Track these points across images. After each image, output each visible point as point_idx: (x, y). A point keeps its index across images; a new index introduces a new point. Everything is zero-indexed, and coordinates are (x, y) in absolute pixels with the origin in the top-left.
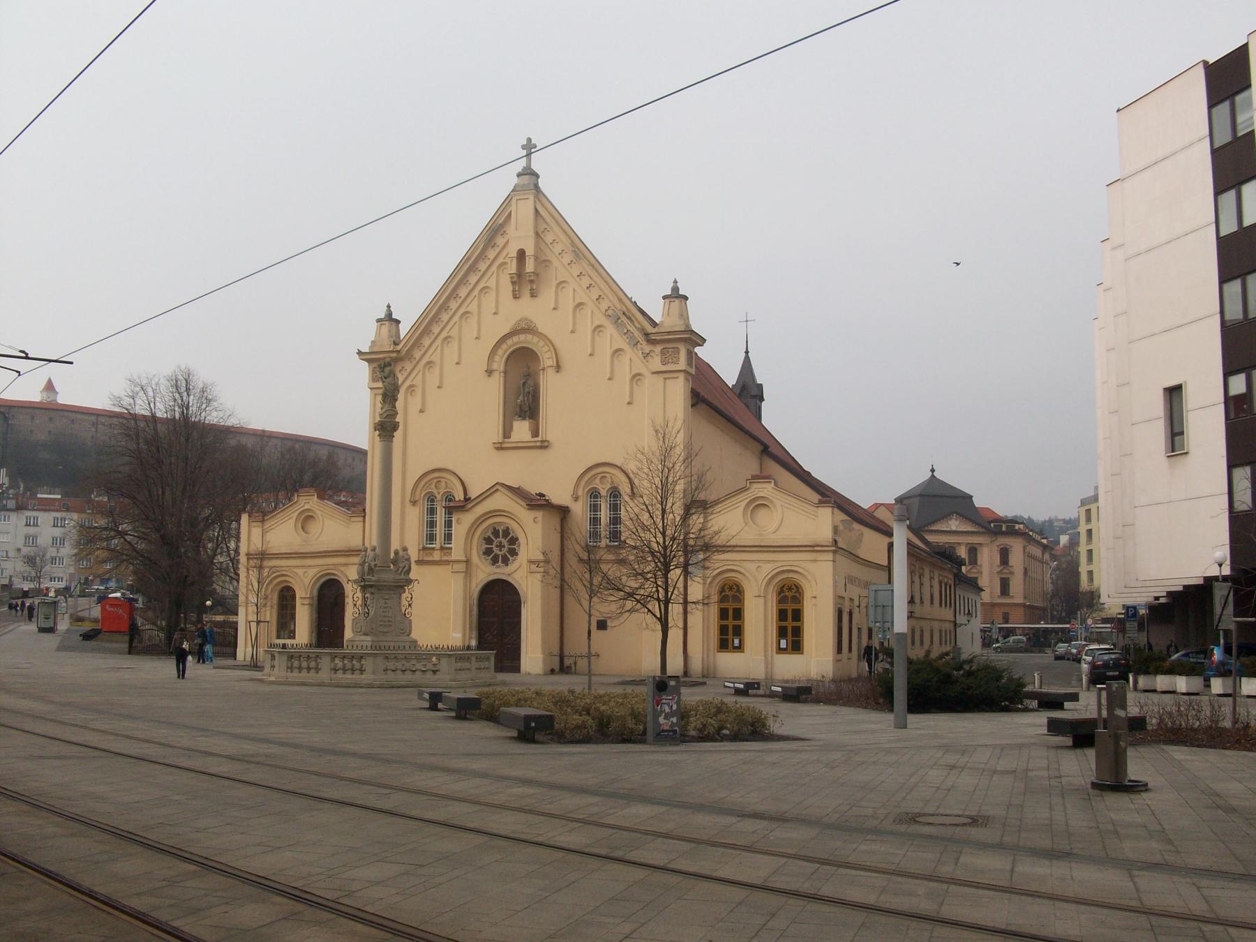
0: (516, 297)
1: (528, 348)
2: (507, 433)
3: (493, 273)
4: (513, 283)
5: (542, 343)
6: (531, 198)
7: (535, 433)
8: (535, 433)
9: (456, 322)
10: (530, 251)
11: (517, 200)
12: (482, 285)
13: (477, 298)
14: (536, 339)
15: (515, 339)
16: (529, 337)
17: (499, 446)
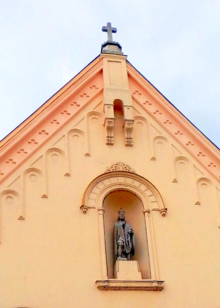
0: (110, 144)
1: (128, 191)
2: (113, 274)
3: (83, 119)
4: (109, 129)
5: (143, 187)
6: (124, 62)
7: (145, 275)
8: (145, 275)
9: (42, 156)
10: (127, 101)
11: (108, 61)
12: (70, 127)
13: (66, 137)
14: (137, 184)
15: (114, 180)
16: (129, 181)
17: (105, 284)
